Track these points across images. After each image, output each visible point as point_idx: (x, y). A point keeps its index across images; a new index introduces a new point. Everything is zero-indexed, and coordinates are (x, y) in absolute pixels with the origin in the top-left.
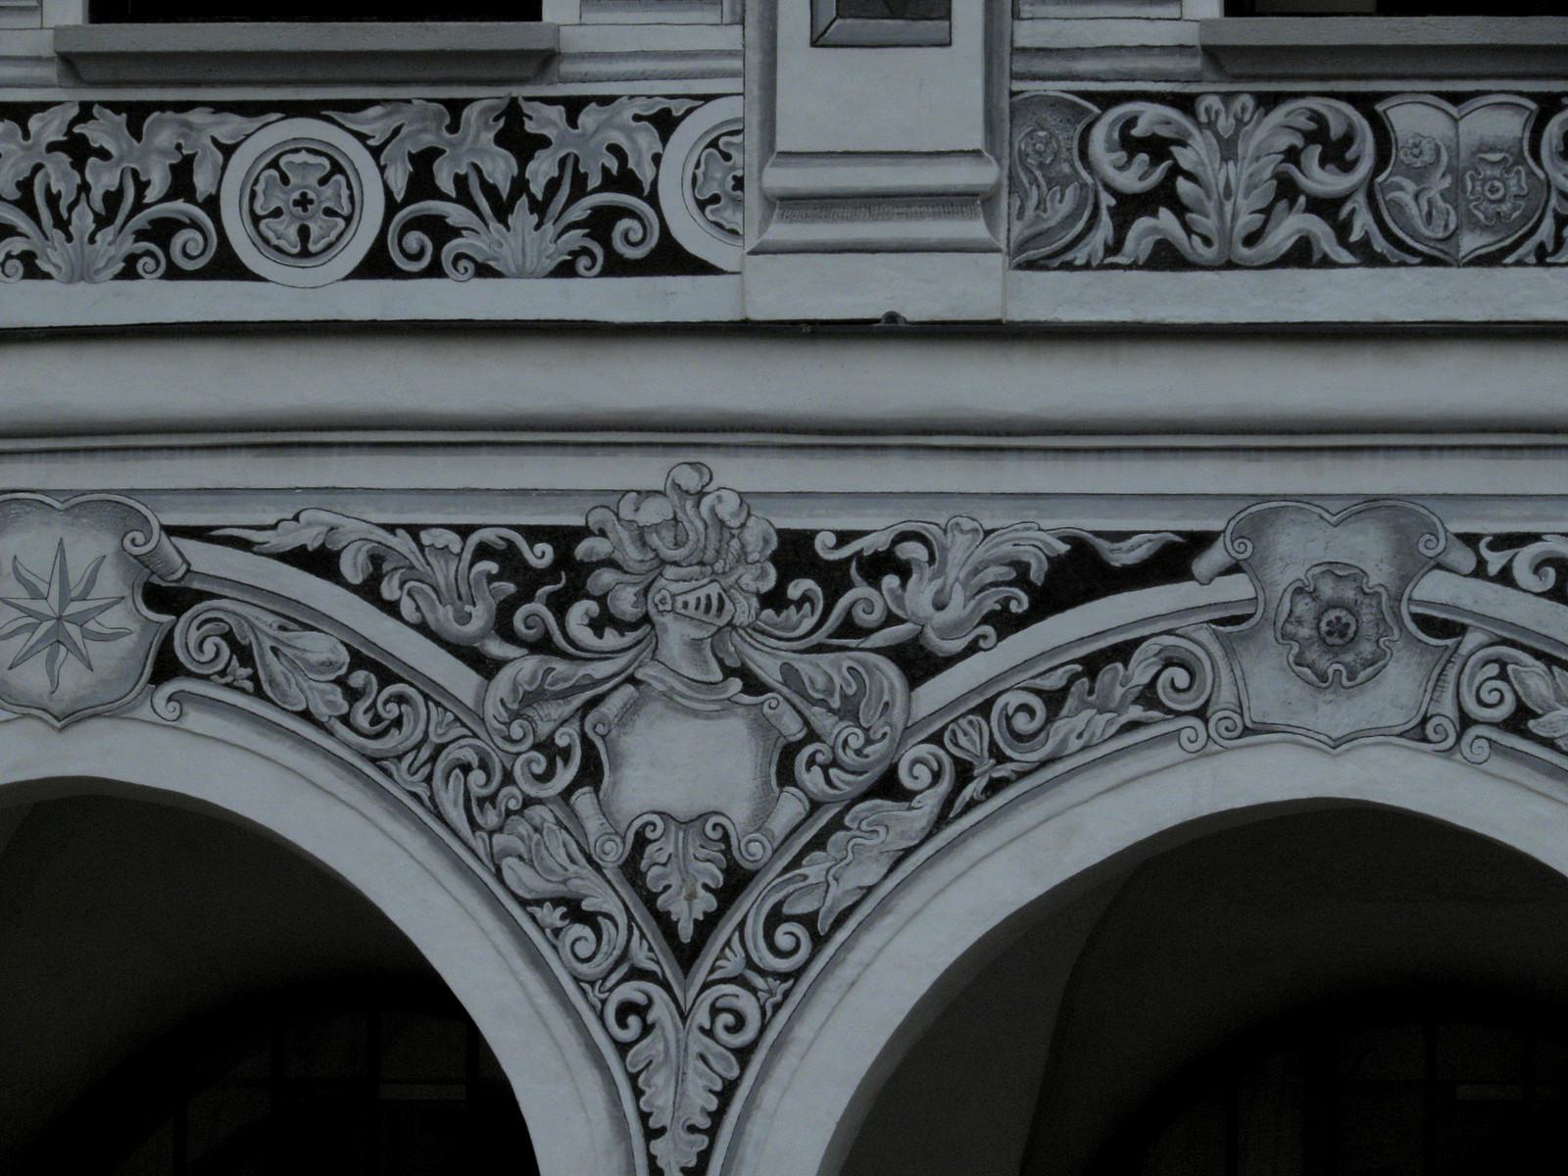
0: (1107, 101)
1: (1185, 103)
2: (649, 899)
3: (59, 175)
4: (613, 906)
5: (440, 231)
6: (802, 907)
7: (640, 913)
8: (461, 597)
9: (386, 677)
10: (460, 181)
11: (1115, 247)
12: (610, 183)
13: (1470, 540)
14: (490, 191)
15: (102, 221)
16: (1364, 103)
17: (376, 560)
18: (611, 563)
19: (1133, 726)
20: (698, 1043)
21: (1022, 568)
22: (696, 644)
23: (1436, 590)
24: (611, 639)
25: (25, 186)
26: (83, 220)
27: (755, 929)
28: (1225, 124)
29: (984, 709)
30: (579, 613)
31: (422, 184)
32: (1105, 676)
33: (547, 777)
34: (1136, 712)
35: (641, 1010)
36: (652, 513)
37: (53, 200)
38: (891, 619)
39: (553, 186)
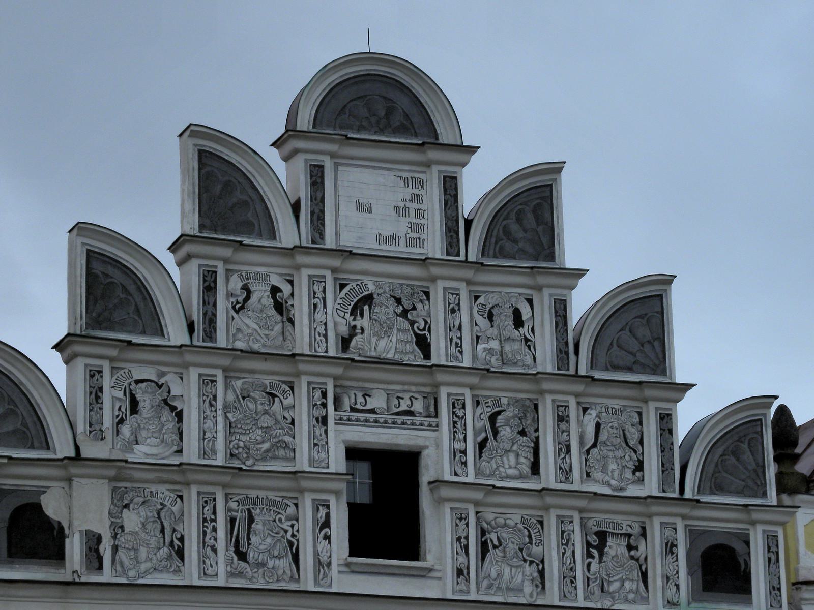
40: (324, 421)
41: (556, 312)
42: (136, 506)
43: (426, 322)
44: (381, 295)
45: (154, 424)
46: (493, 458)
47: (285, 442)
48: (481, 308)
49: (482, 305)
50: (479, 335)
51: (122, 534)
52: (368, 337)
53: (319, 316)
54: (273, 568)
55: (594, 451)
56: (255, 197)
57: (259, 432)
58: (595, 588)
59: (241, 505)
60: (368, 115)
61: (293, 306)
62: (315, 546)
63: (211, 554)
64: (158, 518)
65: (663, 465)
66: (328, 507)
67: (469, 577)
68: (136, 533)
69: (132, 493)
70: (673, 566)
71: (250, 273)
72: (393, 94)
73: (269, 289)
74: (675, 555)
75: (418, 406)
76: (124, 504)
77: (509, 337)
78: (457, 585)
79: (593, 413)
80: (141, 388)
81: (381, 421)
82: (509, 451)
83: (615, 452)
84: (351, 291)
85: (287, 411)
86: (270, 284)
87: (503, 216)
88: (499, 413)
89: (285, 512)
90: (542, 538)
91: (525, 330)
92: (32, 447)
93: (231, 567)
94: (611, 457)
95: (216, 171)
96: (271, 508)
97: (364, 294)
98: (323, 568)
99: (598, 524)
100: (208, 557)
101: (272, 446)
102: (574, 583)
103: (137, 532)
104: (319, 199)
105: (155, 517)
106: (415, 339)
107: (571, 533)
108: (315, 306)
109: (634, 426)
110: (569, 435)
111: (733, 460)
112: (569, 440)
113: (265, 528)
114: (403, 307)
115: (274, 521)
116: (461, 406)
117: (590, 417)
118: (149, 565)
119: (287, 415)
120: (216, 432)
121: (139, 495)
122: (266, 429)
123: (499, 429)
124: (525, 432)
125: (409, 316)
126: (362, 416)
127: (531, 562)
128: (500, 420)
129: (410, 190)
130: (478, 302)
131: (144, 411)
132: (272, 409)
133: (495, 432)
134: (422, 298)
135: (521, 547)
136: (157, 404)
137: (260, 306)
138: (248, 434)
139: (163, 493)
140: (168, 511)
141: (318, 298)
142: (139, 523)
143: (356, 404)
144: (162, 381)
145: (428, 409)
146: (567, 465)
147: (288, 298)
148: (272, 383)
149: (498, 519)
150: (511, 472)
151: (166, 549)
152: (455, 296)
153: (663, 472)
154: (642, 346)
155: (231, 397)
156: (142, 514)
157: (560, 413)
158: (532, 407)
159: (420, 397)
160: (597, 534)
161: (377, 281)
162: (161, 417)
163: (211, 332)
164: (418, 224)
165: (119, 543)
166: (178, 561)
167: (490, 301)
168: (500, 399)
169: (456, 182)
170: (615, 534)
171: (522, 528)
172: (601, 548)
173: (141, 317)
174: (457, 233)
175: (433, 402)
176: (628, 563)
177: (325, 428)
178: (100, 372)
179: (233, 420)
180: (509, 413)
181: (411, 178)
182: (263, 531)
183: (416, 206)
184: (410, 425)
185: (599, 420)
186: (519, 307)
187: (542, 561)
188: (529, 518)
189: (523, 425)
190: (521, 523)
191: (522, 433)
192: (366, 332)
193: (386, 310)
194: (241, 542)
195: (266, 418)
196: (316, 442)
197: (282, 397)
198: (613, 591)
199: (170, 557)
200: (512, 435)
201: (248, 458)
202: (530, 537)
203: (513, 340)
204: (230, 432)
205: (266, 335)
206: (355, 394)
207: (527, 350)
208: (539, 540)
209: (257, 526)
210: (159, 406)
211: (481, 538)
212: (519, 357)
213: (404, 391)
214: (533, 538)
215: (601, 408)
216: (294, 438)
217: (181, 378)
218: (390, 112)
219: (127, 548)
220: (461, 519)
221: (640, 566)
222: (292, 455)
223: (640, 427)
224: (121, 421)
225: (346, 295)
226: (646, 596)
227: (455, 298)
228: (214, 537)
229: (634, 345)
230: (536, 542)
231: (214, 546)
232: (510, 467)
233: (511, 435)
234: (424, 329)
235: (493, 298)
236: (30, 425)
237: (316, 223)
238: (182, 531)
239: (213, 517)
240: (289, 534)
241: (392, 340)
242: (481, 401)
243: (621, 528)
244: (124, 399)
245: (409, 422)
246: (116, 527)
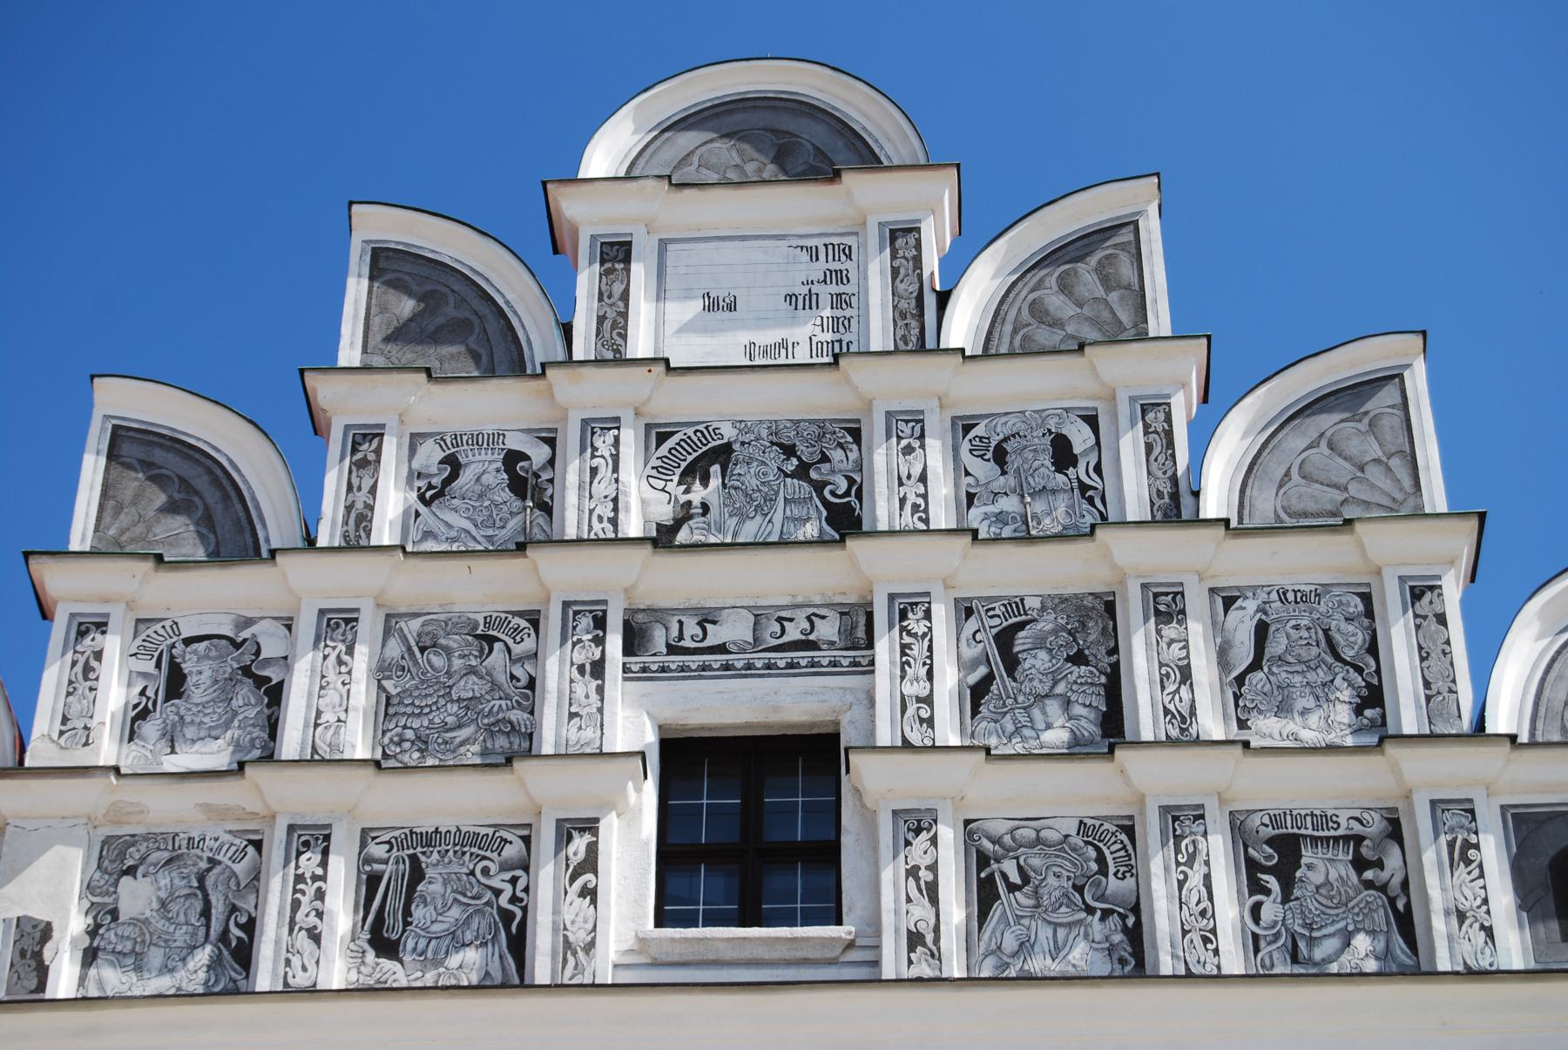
40: (598, 669)
42: (152, 868)
43: (851, 481)
44: (749, 443)
45: (215, 713)
46: (1006, 713)
47: (510, 722)
48: (979, 444)
49: (981, 438)
50: (973, 491)
51: (113, 925)
52: (718, 520)
53: (603, 487)
54: (461, 966)
55: (1257, 677)
58: (1276, 955)
59: (395, 848)
60: (738, 160)
61: (551, 481)
62: (556, 911)
63: (306, 945)
64: (198, 888)
65: (1427, 685)
67: (939, 949)
68: (146, 922)
69: (145, 844)
70: (1472, 889)
71: (461, 435)
72: (787, 123)
73: (502, 456)
74: (1473, 865)
75: (828, 630)
76: (125, 868)
77: (1044, 487)
78: (909, 967)
79: (1251, 605)
80: (195, 652)
81: (739, 664)
82: (1047, 696)
83: (1308, 675)
84: (682, 443)
85: (519, 665)
86: (503, 449)
87: (1031, 285)
88: (1021, 626)
89: (499, 855)
90: (1133, 862)
93: (359, 972)
94: (1298, 685)
95: (407, 278)
96: (465, 849)
97: (710, 446)
98: (575, 954)
99: (1275, 821)
100: (298, 952)
102: (1212, 943)
103: (147, 919)
104: (617, 295)
105: (191, 887)
106: (825, 513)
107: (1200, 838)
108: (594, 471)
109: (1353, 620)
110: (1186, 647)
112: (1188, 656)
113: (449, 891)
114: (799, 458)
115: (472, 873)
116: (921, 614)
117: (1241, 613)
119: (518, 672)
120: (346, 711)
121: (162, 847)
122: (470, 703)
123: (1020, 656)
124: (1086, 657)
125: (814, 475)
126: (694, 661)
127: (1106, 914)
128: (1022, 640)
129: (822, 265)
130: (971, 435)
131: (196, 691)
132: (484, 664)
133: (1012, 663)
134: (842, 441)
135: (1079, 882)
136: (226, 676)
137: (478, 489)
138: (427, 714)
139: (216, 839)
140: (223, 873)
141: (602, 456)
142: (154, 900)
143: (681, 638)
144: (246, 634)
145: (851, 634)
146: (1183, 704)
147: (543, 468)
148: (491, 616)
149: (1019, 832)
151: (208, 948)
152: (911, 424)
153: (1428, 698)
154: (1362, 470)
155: (394, 649)
156: (163, 883)
157: (1162, 608)
158: (1101, 608)
159: (833, 616)
160: (1271, 842)
161: (741, 422)
162: (232, 699)
163: (360, 537)
164: (838, 319)
165: (102, 944)
166: (235, 970)
167: (998, 430)
168: (1022, 600)
169: (917, 236)
170: (1321, 838)
171: (1082, 844)
172: (1287, 871)
173: (214, 527)
175: (862, 621)
176: (1360, 897)
177: (600, 682)
179: (393, 692)
180: (1045, 625)
181: (826, 245)
182: (444, 895)
184: (806, 667)
185: (1264, 617)
186: (1064, 432)
187: (1136, 909)
188: (1097, 823)
189: (1078, 644)
190: (1078, 834)
191: (1078, 659)
192: (714, 511)
194: (389, 921)
195: (471, 682)
196: (573, 710)
197: (510, 641)
198: (1323, 960)
200: (1054, 666)
202: (1101, 860)
203: (1054, 492)
204: (386, 714)
205: (489, 538)
206: (681, 623)
207: (1085, 506)
208: (1126, 866)
209: (432, 887)
210: (231, 679)
211: (978, 874)
214: (1109, 858)
215: (1269, 594)
216: (532, 713)
217: (289, 627)
219: (119, 953)
220: (918, 831)
222: (526, 744)
223: (1366, 622)
224: (143, 714)
225: (670, 452)
226: (1412, 963)
227: (913, 428)
228: (317, 910)
229: (1342, 470)
230: (1118, 871)
231: (315, 927)
233: (1050, 665)
234: (847, 493)
235: (1006, 423)
237: (607, 336)
238: (252, 910)
239: (319, 871)
240: (504, 901)
241: (774, 520)
242: (977, 607)
243: (1335, 826)
244: (156, 672)
245: (803, 663)
246: (99, 912)
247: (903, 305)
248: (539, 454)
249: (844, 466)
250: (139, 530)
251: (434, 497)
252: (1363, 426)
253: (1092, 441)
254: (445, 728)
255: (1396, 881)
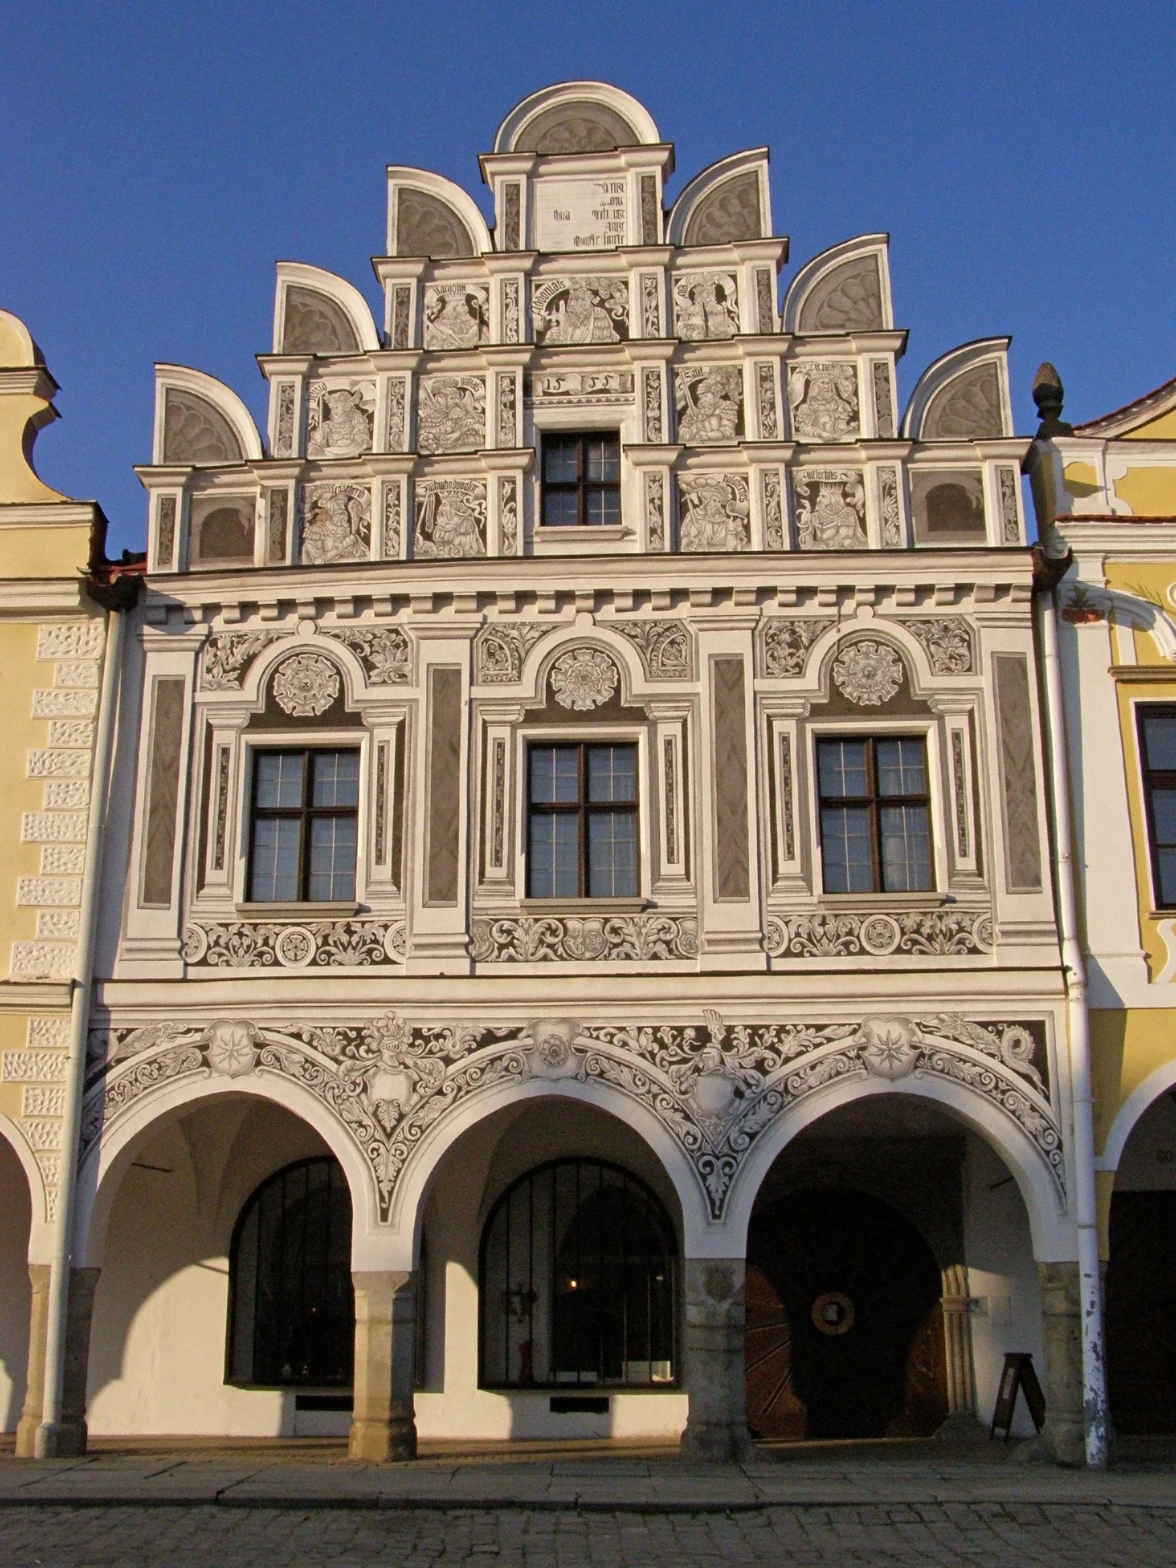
0: (496, 921)
1: (516, 921)
2: (379, 1122)
3: (236, 941)
4: (369, 1123)
5: (330, 954)
6: (418, 1123)
7: (378, 1128)
8: (333, 1046)
9: (314, 1065)
10: (335, 942)
11: (499, 957)
12: (372, 942)
13: (588, 1029)
14: (342, 944)
15: (246, 952)
16: (561, 920)
17: (312, 1036)
18: (370, 1036)
19: (503, 1077)
20: (392, 1158)
21: (475, 1037)
22: (392, 1057)
23: (580, 1041)
24: (370, 1055)
25: (227, 944)
26: (241, 952)
27: (406, 1129)
28: (526, 926)
29: (465, 1073)
30: (363, 1048)
31: (325, 942)
32: (495, 1064)
33: (353, 1091)
34: (503, 1073)
35: (377, 1150)
36: (381, 1023)
37: (234, 947)
38: (441, 1050)
39: (358, 943)
40: (512, 405)
41: (759, 282)
43: (624, 308)
55: (804, 407)
56: (453, 220)
57: (449, 423)
65: (879, 412)
66: (514, 483)
75: (614, 384)
88: (700, 381)
91: (728, 304)
92: (226, 459)
99: (809, 475)
101: (462, 434)
108: (507, 306)
110: (773, 393)
111: (964, 403)
118: (334, 552)
119: (477, 405)
122: (457, 421)
125: (607, 305)
126: (555, 399)
127: (735, 518)
128: (701, 389)
129: (609, 195)
133: (696, 400)
144: (355, 389)
150: (712, 435)
154: (855, 303)
159: (616, 376)
160: (808, 485)
174: (655, 224)
178: (292, 387)
180: (710, 381)
183: (615, 207)
187: (748, 516)
191: (726, 397)
193: (582, 303)
199: (355, 543)
201: (437, 449)
205: (461, 339)
212: (721, 329)
213: (599, 372)
218: (591, 132)
220: (654, 481)
221: (858, 512)
229: (847, 304)
232: (712, 430)
236: (225, 440)
240: (476, 514)
247: (647, 217)
248: (481, 295)
249: (622, 301)
250: (303, 338)
251: (436, 318)
252: (857, 281)
253: (733, 288)
254: (446, 433)
255: (860, 503)
